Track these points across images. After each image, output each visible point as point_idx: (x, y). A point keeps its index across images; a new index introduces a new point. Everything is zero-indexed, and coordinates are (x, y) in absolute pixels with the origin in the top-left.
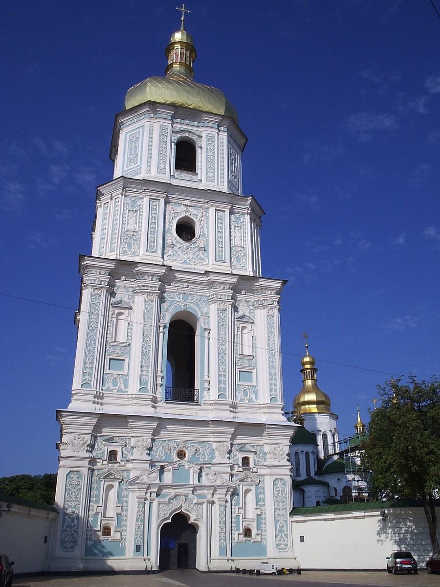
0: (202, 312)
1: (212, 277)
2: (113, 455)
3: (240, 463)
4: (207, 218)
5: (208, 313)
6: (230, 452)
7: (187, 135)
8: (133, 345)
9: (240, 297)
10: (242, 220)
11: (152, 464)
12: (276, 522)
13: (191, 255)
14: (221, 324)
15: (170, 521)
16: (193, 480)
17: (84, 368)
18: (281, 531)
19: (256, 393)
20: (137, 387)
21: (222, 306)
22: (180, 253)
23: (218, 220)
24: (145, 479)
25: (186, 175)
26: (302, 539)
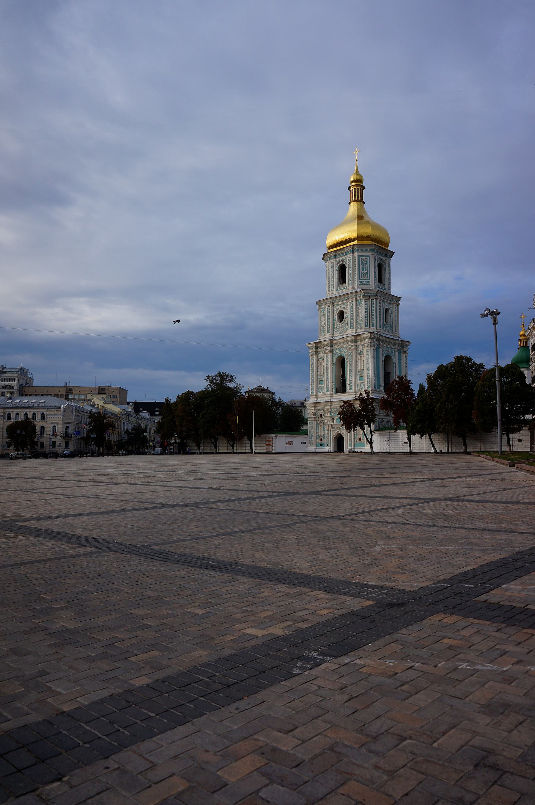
2: (321, 415)
9: (358, 343)
11: (330, 417)
13: (343, 329)
14: (350, 360)
19: (364, 385)
23: (351, 307)
24: (329, 423)
25: (342, 285)
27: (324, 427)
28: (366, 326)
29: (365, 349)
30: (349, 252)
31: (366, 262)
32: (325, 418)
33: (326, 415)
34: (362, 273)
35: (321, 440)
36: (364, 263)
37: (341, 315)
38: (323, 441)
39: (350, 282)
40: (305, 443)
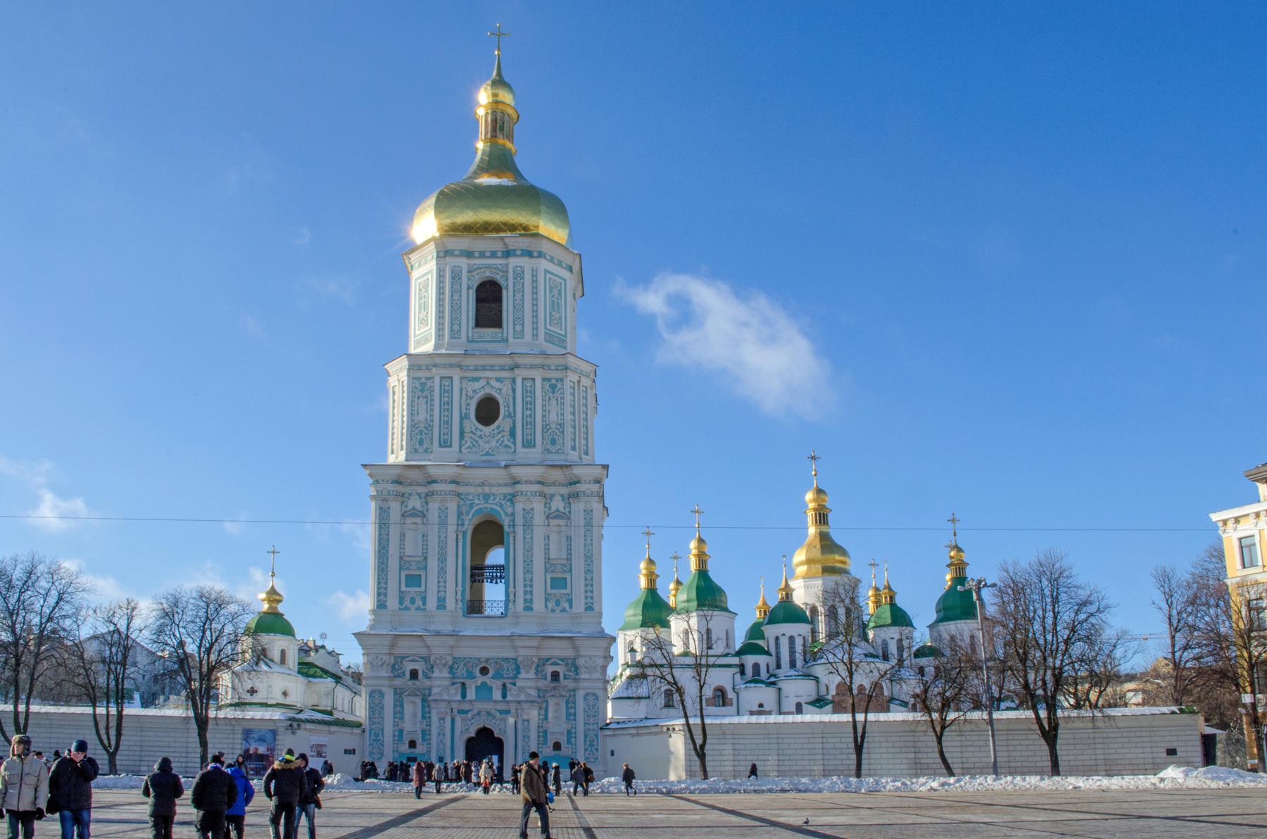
0: (506, 514)
1: (516, 471)
2: (414, 674)
3: (549, 678)
4: (514, 391)
5: (513, 514)
6: (538, 666)
7: (488, 274)
8: (429, 561)
10: (559, 385)
12: (586, 736)
13: (494, 443)
15: (473, 735)
16: (497, 695)
17: (379, 588)
18: (591, 745)
20: (435, 604)
21: (528, 507)
22: (481, 442)
24: (445, 697)
25: (489, 332)
26: (612, 754)
27: (423, 707)
28: (574, 448)
29: (578, 507)
30: (519, 253)
31: (560, 291)
32: (428, 683)
33: (436, 674)
34: (551, 316)
35: (412, 744)
36: (555, 292)
37: (488, 411)
38: (420, 749)
39: (519, 328)
40: (353, 752)
